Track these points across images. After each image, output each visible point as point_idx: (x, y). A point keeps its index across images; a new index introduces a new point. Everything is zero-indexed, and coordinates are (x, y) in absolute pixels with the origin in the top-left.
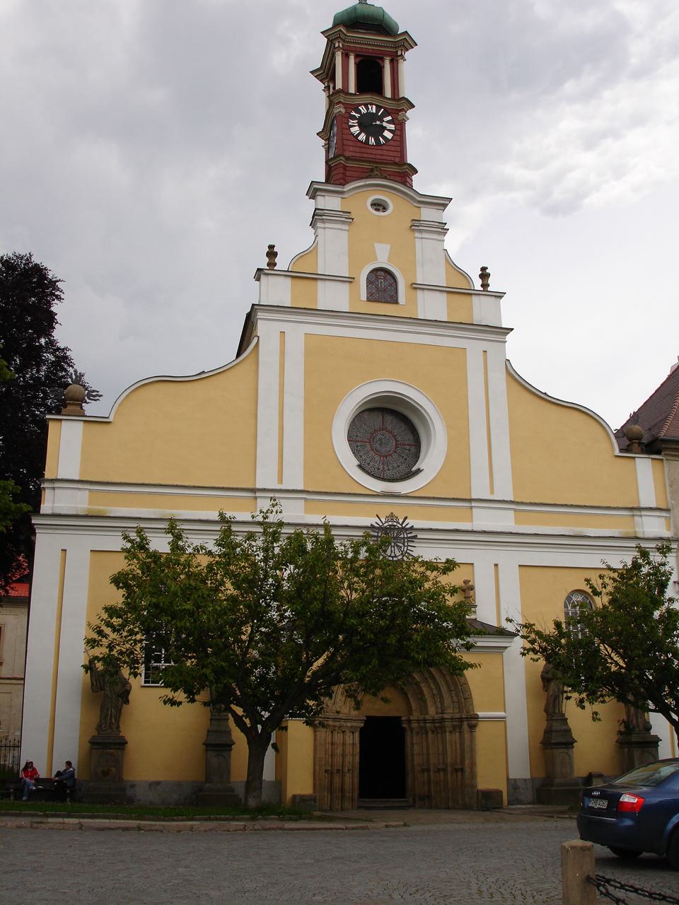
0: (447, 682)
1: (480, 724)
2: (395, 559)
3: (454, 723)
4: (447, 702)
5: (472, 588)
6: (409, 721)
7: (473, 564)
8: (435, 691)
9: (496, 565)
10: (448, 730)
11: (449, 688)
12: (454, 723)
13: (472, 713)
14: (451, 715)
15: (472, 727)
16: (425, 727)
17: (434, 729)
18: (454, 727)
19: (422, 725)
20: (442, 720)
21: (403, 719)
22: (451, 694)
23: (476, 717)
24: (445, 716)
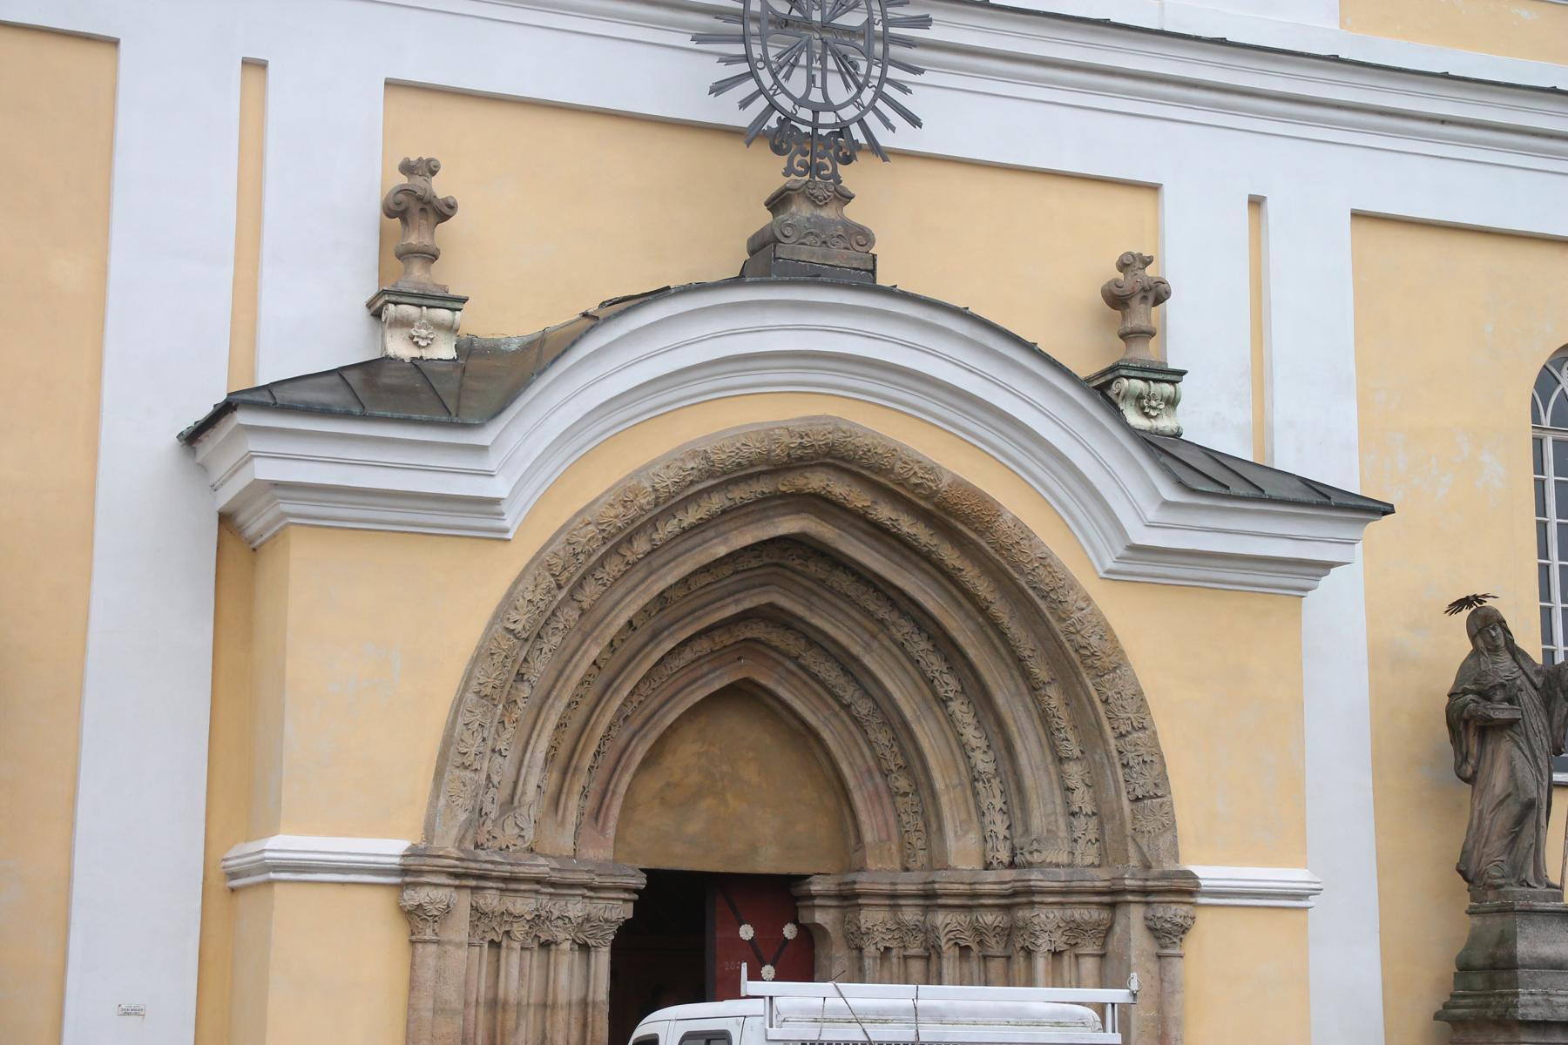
0: (1045, 717)
1: (1203, 917)
2: (827, 118)
3: (1079, 914)
4: (1043, 811)
5: (1157, 294)
6: (848, 899)
7: (1154, 188)
8: (983, 762)
9: (1256, 202)
10: (1044, 944)
11: (1054, 749)
12: (1079, 914)
13: (1169, 866)
14: (1063, 874)
15: (1167, 936)
16: (929, 932)
17: (968, 939)
18: (1075, 930)
19: (910, 915)
20: (1021, 897)
21: (816, 887)
22: (1062, 777)
23: (1185, 889)
24: (1035, 878)
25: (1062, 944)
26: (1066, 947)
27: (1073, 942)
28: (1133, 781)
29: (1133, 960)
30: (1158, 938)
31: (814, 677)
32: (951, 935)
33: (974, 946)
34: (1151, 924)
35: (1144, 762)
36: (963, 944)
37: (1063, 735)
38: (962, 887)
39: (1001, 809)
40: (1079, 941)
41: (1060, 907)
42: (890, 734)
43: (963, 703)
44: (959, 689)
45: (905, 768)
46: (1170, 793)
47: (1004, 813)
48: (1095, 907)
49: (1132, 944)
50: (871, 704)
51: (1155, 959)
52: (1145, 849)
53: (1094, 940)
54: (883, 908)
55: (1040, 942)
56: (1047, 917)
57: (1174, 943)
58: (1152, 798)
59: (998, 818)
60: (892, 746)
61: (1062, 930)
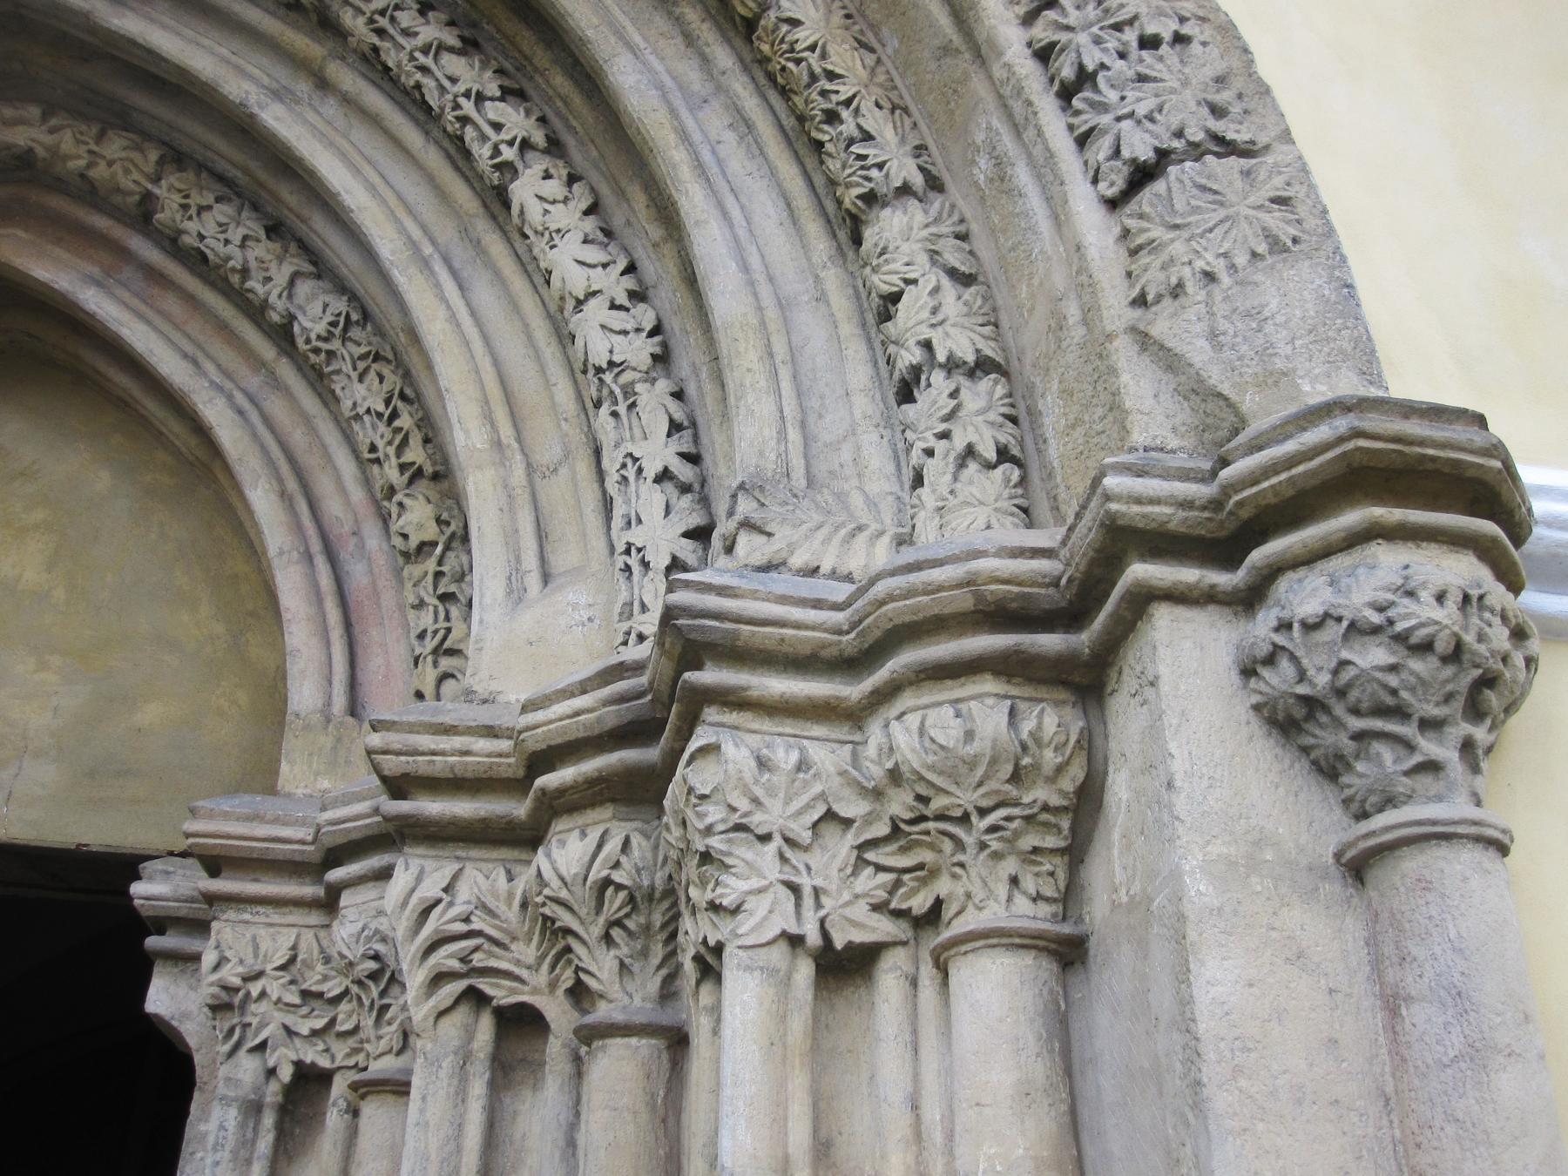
25: (860, 911)
26: (882, 928)
27: (920, 903)
28: (1106, 119)
29: (1199, 889)
30: (1330, 770)
31: (197, 261)
32: (445, 957)
33: (556, 1011)
34: (1279, 678)
35: (1149, 43)
36: (501, 993)
37: (848, 127)
38: (482, 744)
39: (664, 476)
40: (943, 886)
41: (842, 732)
42: (393, 381)
43: (547, 176)
44: (539, 138)
45: (436, 477)
46: (1286, 136)
47: (685, 489)
48: (988, 685)
49: (1181, 804)
50: (340, 305)
51: (1335, 887)
52: (1198, 352)
53: (1010, 866)
54: (297, 916)
55: (731, 889)
56: (763, 764)
57: (1432, 767)
58: (1196, 151)
59: (651, 499)
60: (394, 415)
61: (851, 838)
